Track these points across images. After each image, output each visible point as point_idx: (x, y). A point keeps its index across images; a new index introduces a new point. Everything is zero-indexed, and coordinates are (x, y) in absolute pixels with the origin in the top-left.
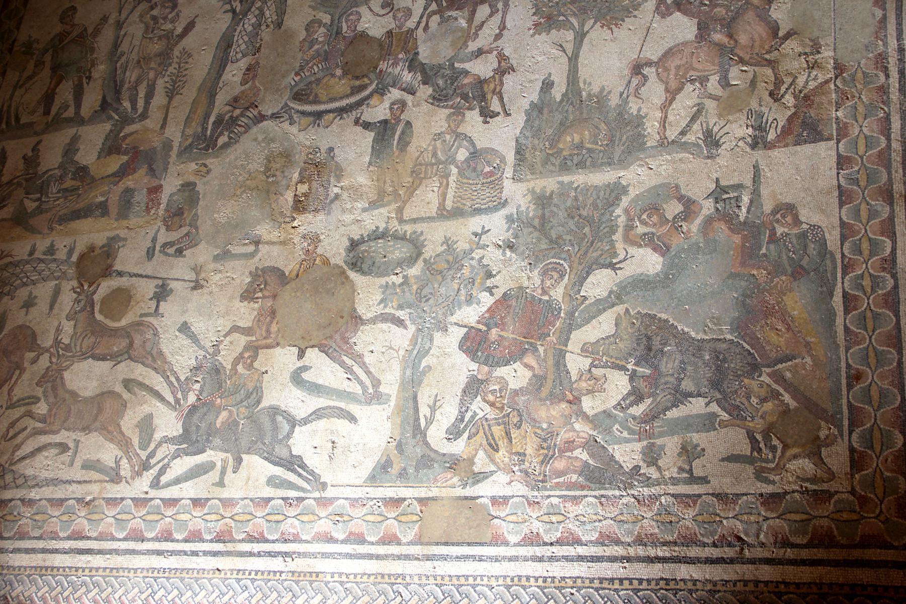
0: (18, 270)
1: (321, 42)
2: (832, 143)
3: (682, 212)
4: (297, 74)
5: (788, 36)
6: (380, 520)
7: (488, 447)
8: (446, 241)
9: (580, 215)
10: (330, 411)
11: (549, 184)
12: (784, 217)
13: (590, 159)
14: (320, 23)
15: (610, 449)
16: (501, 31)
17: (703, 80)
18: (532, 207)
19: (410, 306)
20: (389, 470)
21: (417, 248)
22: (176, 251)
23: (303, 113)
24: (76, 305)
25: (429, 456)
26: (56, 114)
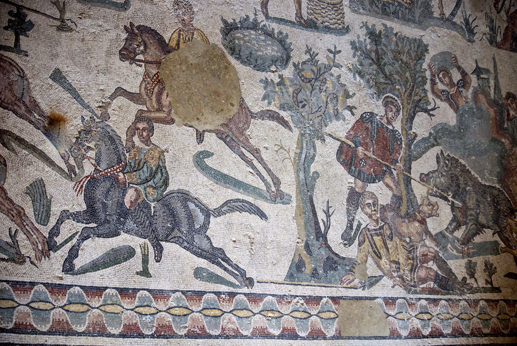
6: (305, 317)
7: (373, 254)
8: (308, 51)
10: (241, 204)
15: (448, 262)
18: (368, 41)
19: (290, 108)
20: (303, 269)
21: (286, 49)
25: (333, 259)
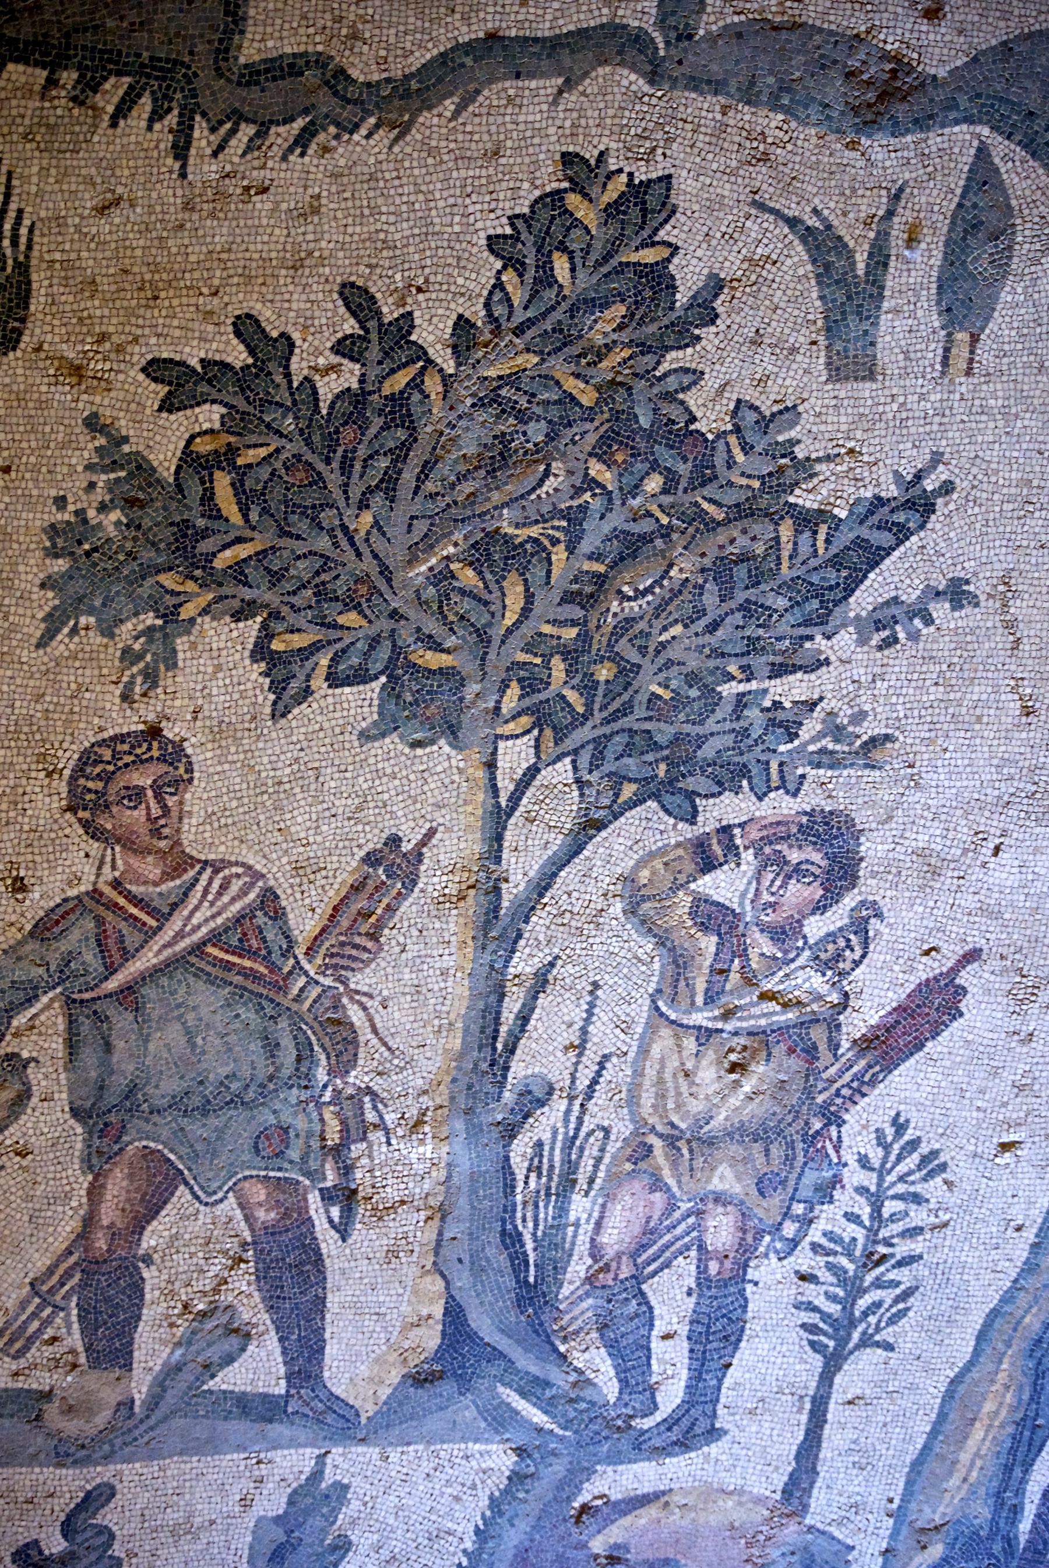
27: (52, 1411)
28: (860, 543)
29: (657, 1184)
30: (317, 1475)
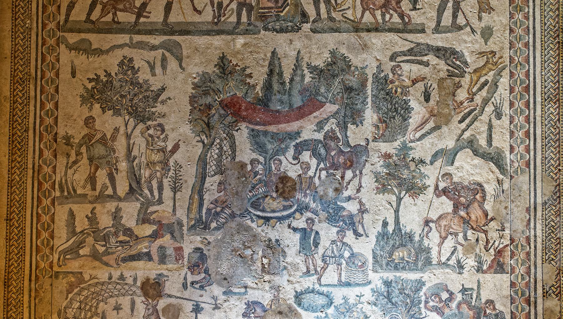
0: (104, 288)
1: (261, 174)
2: (509, 275)
3: (449, 298)
4: (250, 192)
5: (492, 219)
8: (344, 298)
9: (405, 293)
11: (390, 276)
12: (490, 306)
13: (407, 266)
14: (259, 162)
16: (359, 188)
17: (456, 235)
18: (383, 286)
22: (200, 286)
23: (258, 216)
24: (147, 311)
26: (101, 191)
27: (88, 196)
28: (158, 94)
29: (150, 169)
30: (118, 206)
